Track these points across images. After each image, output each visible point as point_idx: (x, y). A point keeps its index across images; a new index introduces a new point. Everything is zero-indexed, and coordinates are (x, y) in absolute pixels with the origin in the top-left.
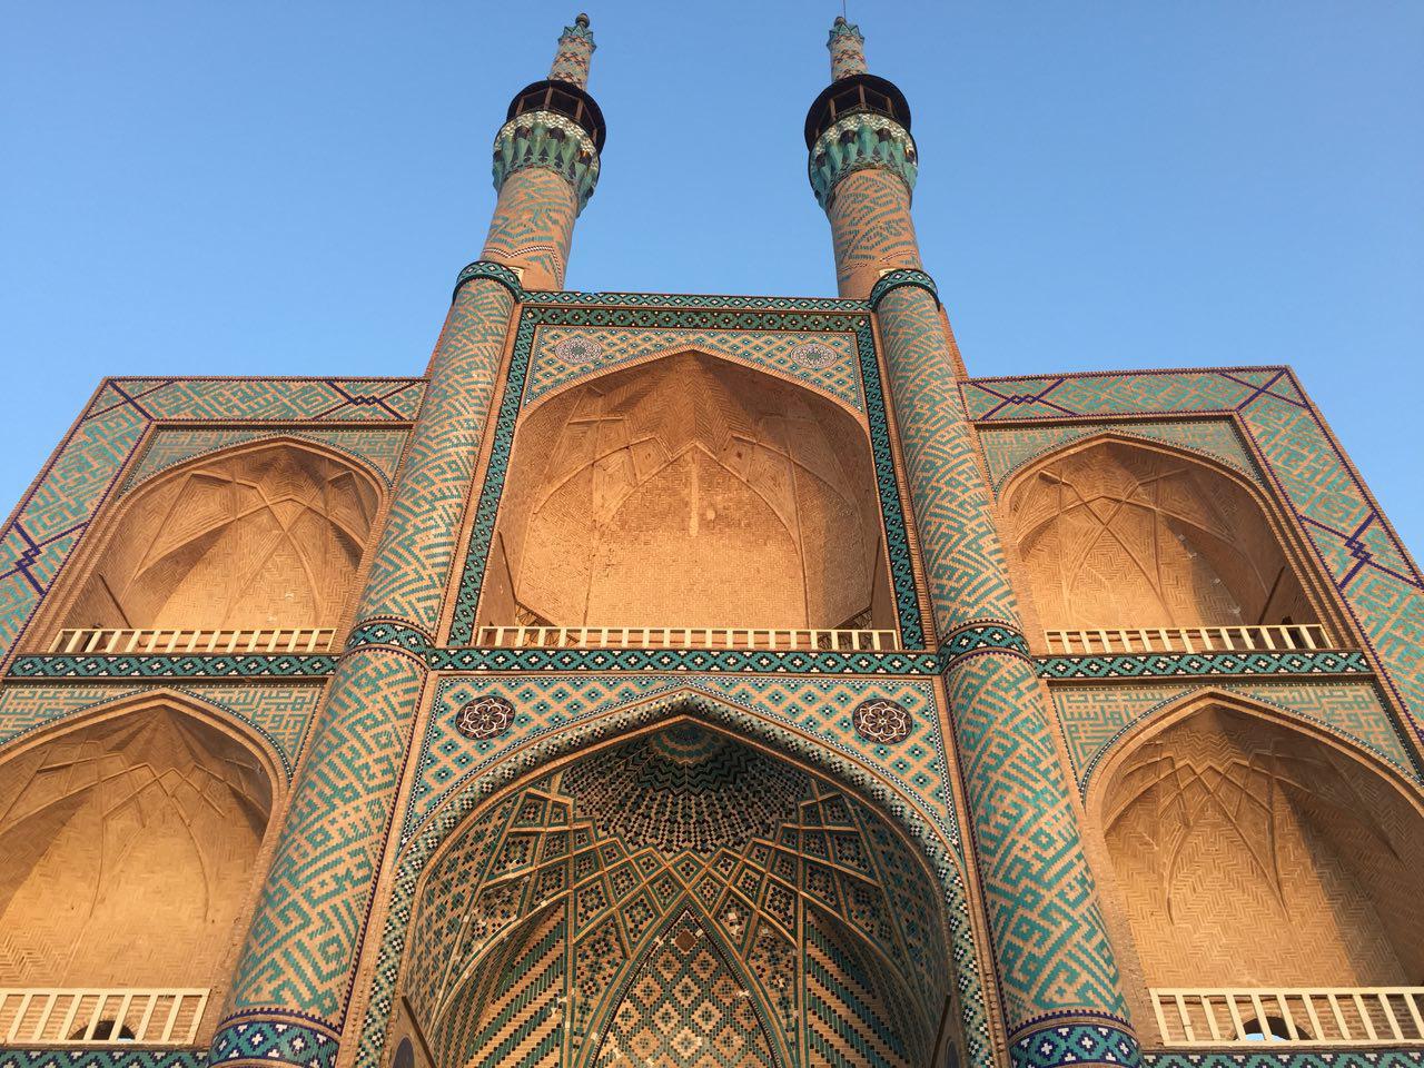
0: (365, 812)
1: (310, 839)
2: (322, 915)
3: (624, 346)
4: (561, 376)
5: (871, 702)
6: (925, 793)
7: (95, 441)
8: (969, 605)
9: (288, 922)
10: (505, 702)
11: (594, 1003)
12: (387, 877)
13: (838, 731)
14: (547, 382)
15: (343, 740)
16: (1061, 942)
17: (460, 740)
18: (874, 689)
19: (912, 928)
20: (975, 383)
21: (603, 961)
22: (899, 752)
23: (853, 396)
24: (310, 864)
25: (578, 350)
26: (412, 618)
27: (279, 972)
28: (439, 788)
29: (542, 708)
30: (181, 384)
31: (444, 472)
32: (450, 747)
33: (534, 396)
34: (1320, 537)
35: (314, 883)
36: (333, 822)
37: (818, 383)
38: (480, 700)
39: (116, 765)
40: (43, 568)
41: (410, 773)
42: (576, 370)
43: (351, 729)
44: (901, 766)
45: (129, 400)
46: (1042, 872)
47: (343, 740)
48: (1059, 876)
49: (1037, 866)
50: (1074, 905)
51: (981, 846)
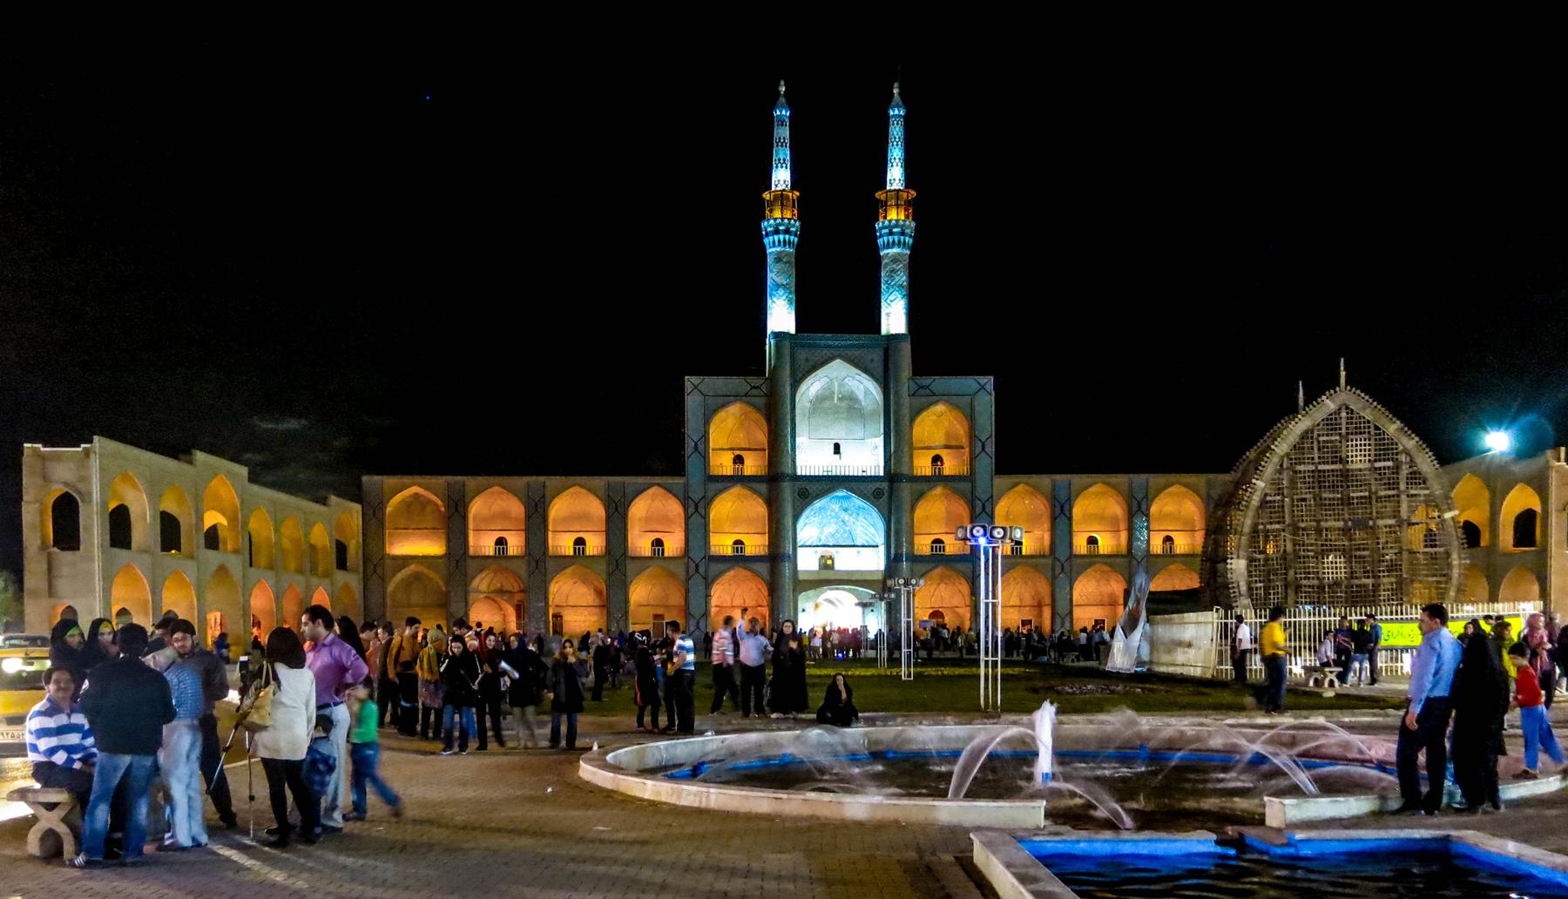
18: (877, 485)
40: (701, 447)
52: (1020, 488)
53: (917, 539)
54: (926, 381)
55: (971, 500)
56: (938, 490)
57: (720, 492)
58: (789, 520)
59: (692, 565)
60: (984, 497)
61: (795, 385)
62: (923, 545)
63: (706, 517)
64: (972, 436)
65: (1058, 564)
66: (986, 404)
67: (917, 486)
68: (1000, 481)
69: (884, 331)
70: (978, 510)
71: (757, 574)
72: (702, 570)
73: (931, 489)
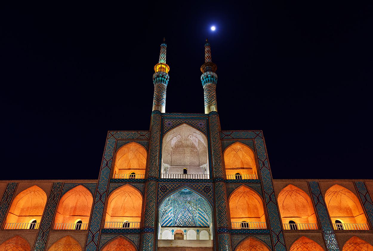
0: (153, 203)
1: (149, 207)
2: (151, 216)
4: (167, 129)
5: (206, 187)
7: (110, 143)
8: (217, 174)
9: (148, 217)
10: (166, 186)
11: (175, 216)
13: (202, 191)
15: (150, 194)
16: (222, 220)
17: (161, 192)
19: (209, 212)
21: (176, 212)
22: (209, 194)
24: (149, 210)
25: (169, 124)
26: (155, 176)
27: (148, 223)
28: (160, 198)
29: (170, 188)
31: (155, 152)
32: (160, 193)
34: (260, 161)
35: (150, 212)
36: (151, 205)
38: (163, 186)
40: (109, 165)
41: (157, 197)
42: (169, 128)
43: (150, 192)
44: (209, 195)
45: (112, 135)
46: (222, 211)
47: (150, 194)
48: (223, 212)
49: (221, 210)
50: (224, 215)
52: (288, 188)
53: (232, 220)
54: (228, 133)
55: (262, 194)
56: (242, 189)
57: (116, 188)
58: (153, 204)
59: (91, 235)
60: (270, 192)
61: (163, 134)
62: (236, 224)
63: (105, 205)
64: (257, 159)
66: (261, 143)
67: (231, 186)
68: (278, 183)
69: (206, 112)
71: (130, 241)
72: (96, 239)
73: (237, 187)
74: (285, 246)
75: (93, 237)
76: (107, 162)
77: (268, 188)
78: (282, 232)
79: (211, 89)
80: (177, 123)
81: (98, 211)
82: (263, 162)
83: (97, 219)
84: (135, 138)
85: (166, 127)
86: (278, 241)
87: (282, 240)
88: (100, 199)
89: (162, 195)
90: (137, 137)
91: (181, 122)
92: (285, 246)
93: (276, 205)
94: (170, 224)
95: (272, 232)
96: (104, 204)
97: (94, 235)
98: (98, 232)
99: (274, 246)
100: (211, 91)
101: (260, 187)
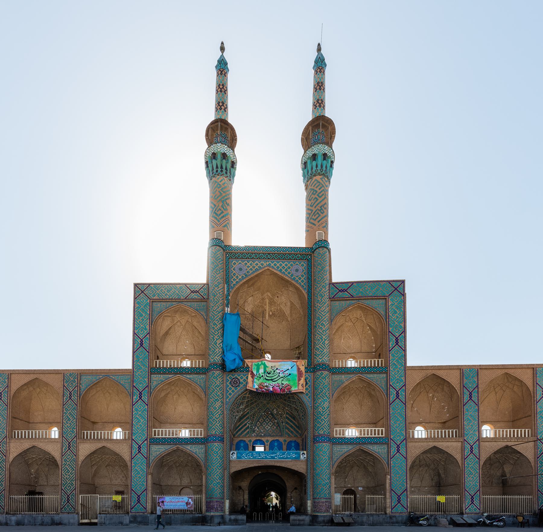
3: (251, 267)
4: (237, 280)
6: (307, 397)
12: (225, 413)
14: (234, 282)
20: (333, 284)
23: (305, 287)
25: (241, 269)
28: (230, 397)
30: (152, 286)
33: (232, 288)
34: (391, 337)
37: (297, 281)
39: (173, 388)
40: (146, 345)
42: (241, 277)
45: (142, 292)
51: (314, 408)
59: (135, 446)
60: (398, 386)
65: (468, 447)
70: (393, 396)
72: (144, 450)
74: (406, 458)
75: (139, 447)
76: (142, 340)
77: (398, 380)
78: (405, 441)
79: (319, 189)
80: (254, 267)
81: (140, 415)
82: (397, 338)
83: (141, 426)
84: (182, 298)
85: (234, 274)
86: (398, 452)
87: (403, 450)
88: (140, 398)
89: (233, 391)
90: (185, 295)
91: (262, 265)
92: (406, 458)
93: (405, 404)
94: (245, 432)
95: (392, 441)
96: (147, 405)
97: (140, 446)
98: (146, 442)
99: (391, 459)
100: (320, 195)
101: (385, 379)
